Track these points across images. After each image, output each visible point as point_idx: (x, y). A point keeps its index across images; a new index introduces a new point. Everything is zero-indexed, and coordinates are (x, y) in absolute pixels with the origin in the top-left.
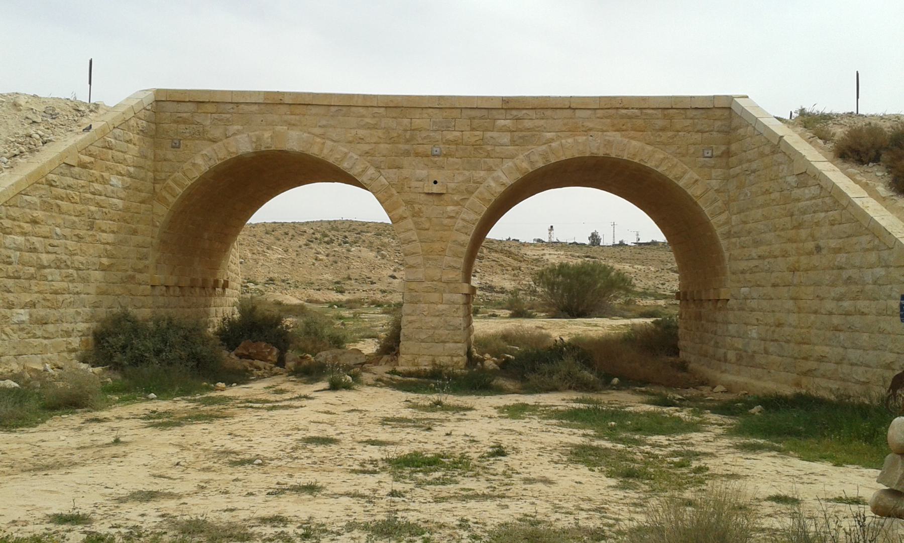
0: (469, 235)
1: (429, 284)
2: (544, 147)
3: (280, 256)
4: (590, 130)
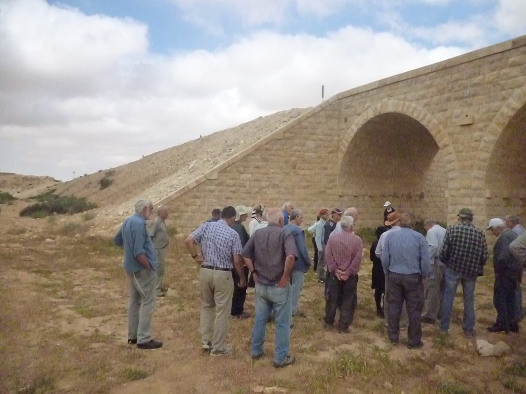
0: (489, 153)
1: (462, 191)
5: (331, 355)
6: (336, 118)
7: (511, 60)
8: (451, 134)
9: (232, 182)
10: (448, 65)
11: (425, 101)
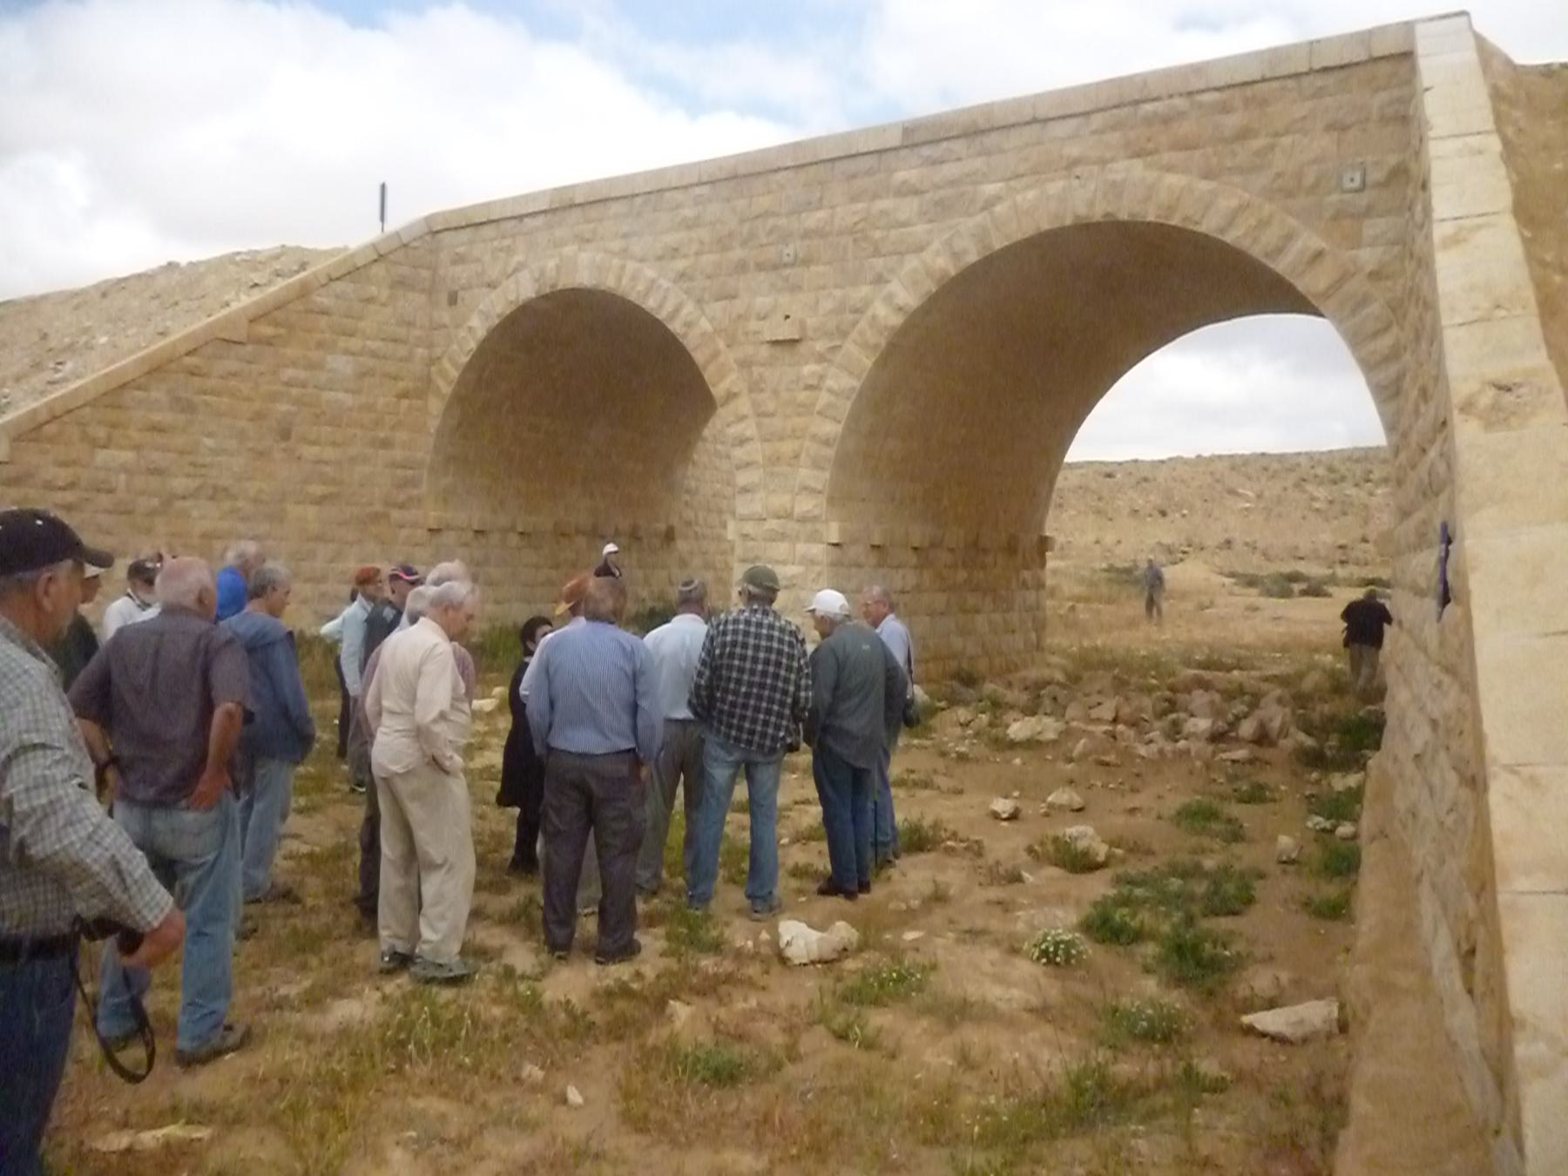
0: (839, 422)
1: (773, 524)
2: (979, 218)
3: (1248, 505)
4: (1076, 162)
5: (365, 1007)
6: (422, 291)
7: (900, 176)
8: (745, 364)
9: (63, 476)
10: (742, 170)
11: (680, 264)
